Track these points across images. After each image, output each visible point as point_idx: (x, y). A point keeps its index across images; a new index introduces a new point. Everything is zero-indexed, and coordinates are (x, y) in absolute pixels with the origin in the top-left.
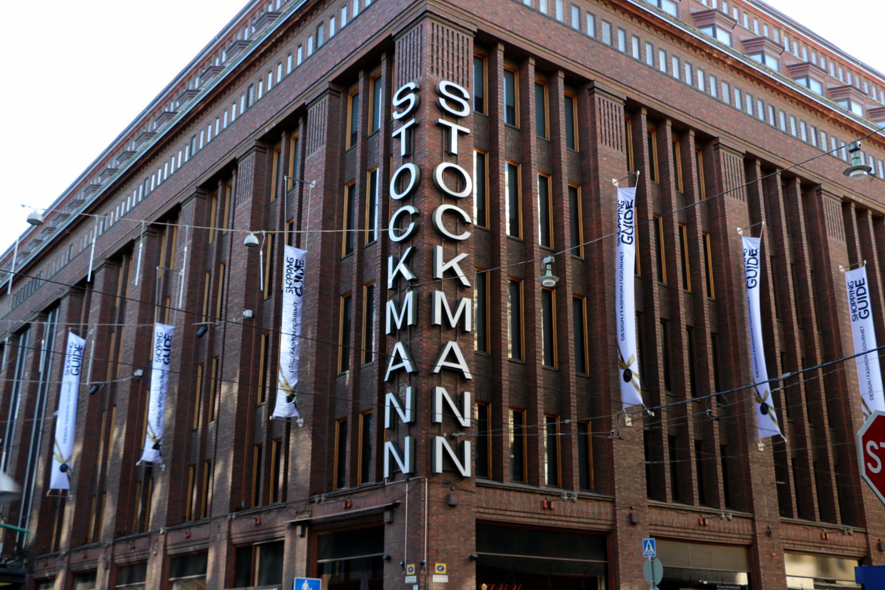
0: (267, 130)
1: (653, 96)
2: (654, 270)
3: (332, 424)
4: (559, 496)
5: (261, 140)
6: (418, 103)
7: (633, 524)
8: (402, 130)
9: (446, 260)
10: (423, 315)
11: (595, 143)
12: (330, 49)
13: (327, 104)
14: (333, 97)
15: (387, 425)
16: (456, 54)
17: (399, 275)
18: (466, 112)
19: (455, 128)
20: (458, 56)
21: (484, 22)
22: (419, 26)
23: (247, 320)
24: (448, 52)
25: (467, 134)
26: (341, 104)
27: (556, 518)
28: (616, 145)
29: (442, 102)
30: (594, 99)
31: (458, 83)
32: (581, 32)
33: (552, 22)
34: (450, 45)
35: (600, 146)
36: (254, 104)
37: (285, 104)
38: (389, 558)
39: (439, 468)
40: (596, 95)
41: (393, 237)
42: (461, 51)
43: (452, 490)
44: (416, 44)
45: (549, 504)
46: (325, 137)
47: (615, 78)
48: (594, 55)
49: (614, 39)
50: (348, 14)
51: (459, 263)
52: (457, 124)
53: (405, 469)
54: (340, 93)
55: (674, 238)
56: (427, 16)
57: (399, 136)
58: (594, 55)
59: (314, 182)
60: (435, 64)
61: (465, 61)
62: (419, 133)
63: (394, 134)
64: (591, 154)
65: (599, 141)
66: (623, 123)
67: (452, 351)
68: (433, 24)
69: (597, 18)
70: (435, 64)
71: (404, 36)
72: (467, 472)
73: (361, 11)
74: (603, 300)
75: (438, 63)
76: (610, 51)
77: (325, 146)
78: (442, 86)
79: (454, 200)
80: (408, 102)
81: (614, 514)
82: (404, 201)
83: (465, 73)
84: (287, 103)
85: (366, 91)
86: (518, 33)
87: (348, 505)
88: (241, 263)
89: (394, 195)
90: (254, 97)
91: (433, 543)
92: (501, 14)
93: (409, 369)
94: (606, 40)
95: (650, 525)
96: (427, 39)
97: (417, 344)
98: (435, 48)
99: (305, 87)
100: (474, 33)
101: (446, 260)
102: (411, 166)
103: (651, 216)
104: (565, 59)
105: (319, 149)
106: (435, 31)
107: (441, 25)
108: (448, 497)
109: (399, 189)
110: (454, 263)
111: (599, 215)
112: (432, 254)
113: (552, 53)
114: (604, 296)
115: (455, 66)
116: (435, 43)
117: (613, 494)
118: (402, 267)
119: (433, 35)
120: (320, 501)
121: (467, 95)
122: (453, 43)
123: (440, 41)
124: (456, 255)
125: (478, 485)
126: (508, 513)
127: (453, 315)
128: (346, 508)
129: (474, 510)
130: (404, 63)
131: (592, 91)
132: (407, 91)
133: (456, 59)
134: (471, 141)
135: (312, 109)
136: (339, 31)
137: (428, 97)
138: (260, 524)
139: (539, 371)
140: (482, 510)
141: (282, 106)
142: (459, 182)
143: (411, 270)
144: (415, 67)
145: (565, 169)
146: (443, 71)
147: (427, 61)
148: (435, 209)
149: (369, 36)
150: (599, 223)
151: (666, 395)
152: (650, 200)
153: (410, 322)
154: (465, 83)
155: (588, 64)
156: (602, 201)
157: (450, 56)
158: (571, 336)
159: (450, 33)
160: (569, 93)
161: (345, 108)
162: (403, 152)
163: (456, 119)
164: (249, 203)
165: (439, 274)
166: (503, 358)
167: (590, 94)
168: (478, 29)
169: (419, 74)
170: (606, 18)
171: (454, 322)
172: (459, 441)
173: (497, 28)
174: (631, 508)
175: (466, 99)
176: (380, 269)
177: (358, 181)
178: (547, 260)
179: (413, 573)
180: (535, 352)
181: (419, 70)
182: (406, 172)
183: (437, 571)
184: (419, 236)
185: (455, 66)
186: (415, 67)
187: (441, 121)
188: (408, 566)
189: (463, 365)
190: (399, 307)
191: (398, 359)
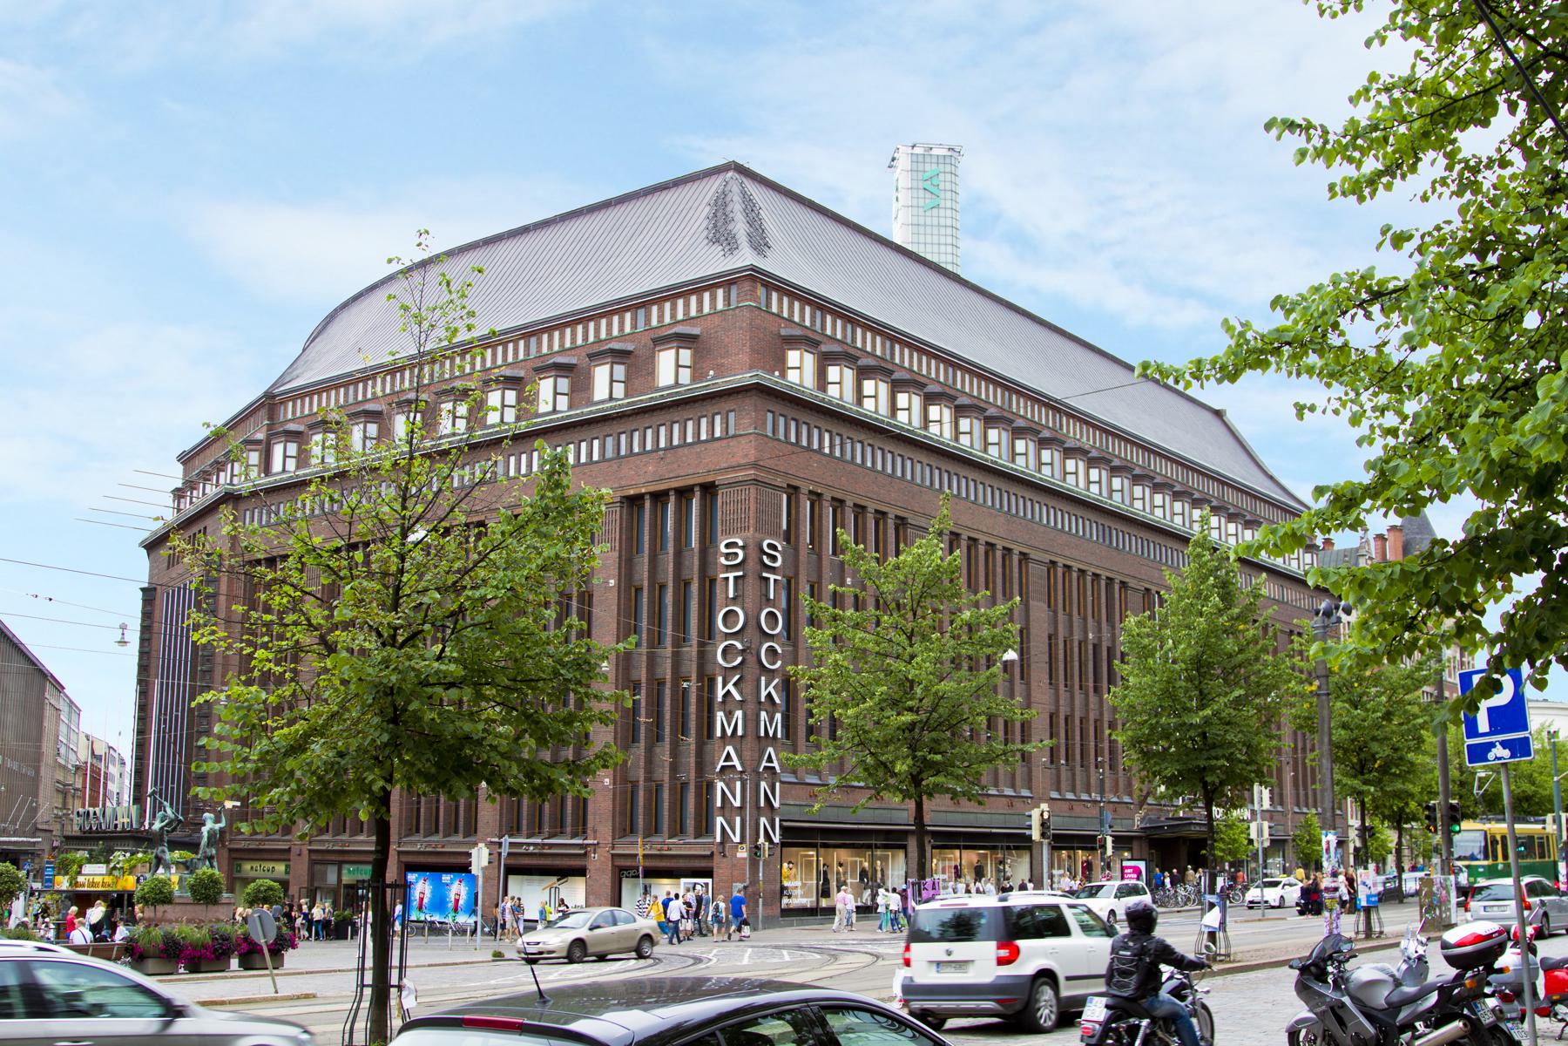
10: (751, 725)
18: (778, 564)
19: (772, 577)
57: (727, 579)
93: (739, 768)
110: (771, 689)
118: (730, 687)
153: (740, 732)
162: (731, 595)
163: (773, 570)
165: (763, 699)
189: (776, 764)
191: (728, 757)
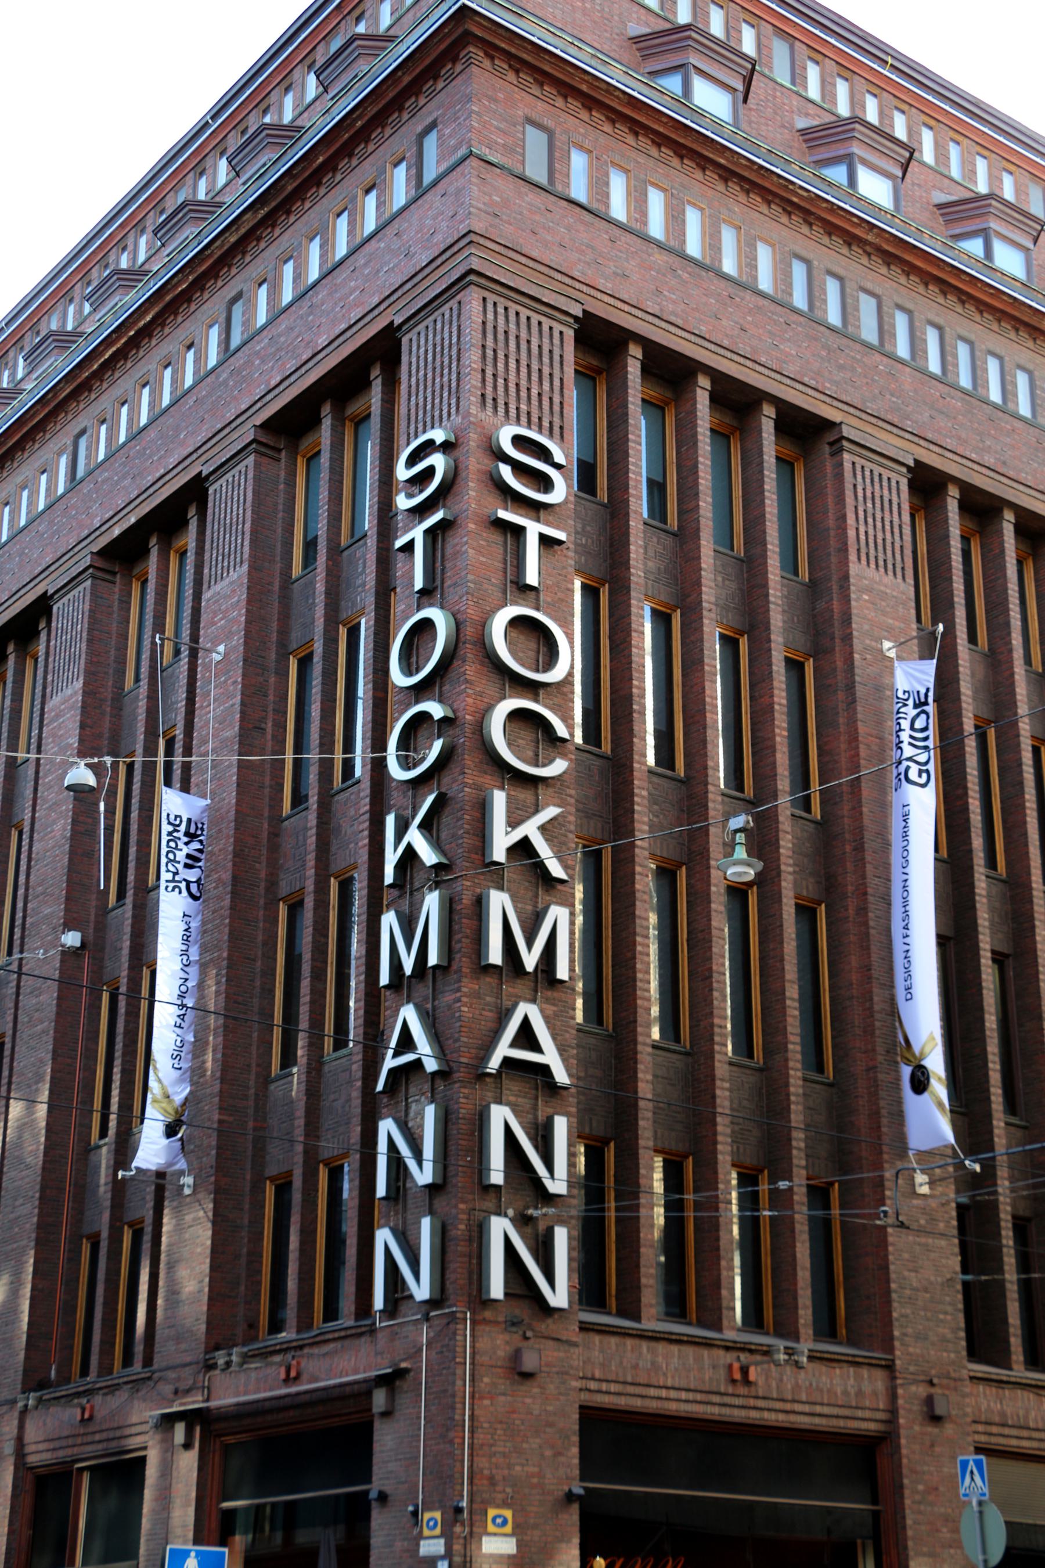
0: (117, 532)
1: (973, 456)
2: (977, 842)
3: (257, 1187)
4: (767, 1352)
5: (102, 553)
6: (451, 475)
7: (936, 1419)
8: (417, 534)
9: (513, 823)
10: (463, 944)
11: (845, 562)
12: (258, 353)
13: (251, 475)
14: (265, 460)
15: (381, 1191)
16: (535, 367)
17: (410, 855)
18: (558, 494)
19: (533, 529)
20: (540, 370)
21: (599, 295)
22: (453, 303)
23: (70, 955)
24: (518, 361)
25: (560, 542)
26: (282, 474)
27: (760, 1403)
28: (890, 566)
29: (506, 472)
30: (842, 464)
31: (540, 431)
32: (813, 317)
33: (748, 295)
34: (524, 346)
35: (854, 568)
36: (89, 473)
37: (158, 475)
38: (383, 1498)
39: (497, 1289)
40: (846, 456)
41: (396, 771)
42: (546, 360)
43: (526, 1338)
44: (446, 343)
45: (745, 1371)
46: (247, 549)
47: (889, 418)
48: (841, 368)
49: (885, 330)
50: (297, 277)
51: (543, 829)
52: (538, 520)
53: (421, 1290)
54: (279, 451)
55: (1021, 772)
56: (471, 283)
57: (409, 547)
58: (841, 368)
59: (221, 648)
60: (489, 389)
61: (557, 383)
62: (454, 541)
63: (399, 543)
64: (835, 588)
65: (853, 557)
66: (906, 518)
67: (526, 1023)
68: (484, 299)
69: (848, 284)
70: (489, 389)
71: (421, 327)
72: (559, 1297)
73: (325, 270)
74: (863, 910)
75: (495, 387)
76: (877, 357)
77: (245, 567)
78: (505, 438)
79: (532, 688)
80: (430, 471)
81: (893, 1396)
82: (420, 691)
83: (556, 408)
84: (162, 471)
85: (337, 446)
86: (672, 319)
87: (293, 1374)
88: (58, 827)
89: (398, 678)
90: (88, 457)
91: (482, 1462)
92: (635, 277)
94: (869, 332)
95: (975, 1422)
96: (472, 335)
97: (449, 1007)
98: (490, 353)
99: (200, 438)
100: (576, 318)
101: (513, 823)
102: (434, 613)
103: (969, 725)
104: (778, 377)
105: (234, 575)
106: (490, 316)
107: (502, 302)
108: (516, 1356)
109: (410, 662)
110: (530, 829)
111: (852, 722)
112: (483, 808)
113: (748, 363)
114: (865, 901)
115: (534, 392)
116: (490, 342)
117: (891, 1350)
118: (415, 837)
119: (484, 323)
120: (228, 1364)
121: (559, 457)
122: (529, 342)
123: (501, 337)
124: (537, 811)
125: (585, 1328)
126: (652, 1392)
127: (530, 943)
128: (287, 1380)
129: (576, 1384)
130: (421, 387)
131: (837, 445)
132: (428, 447)
133: (535, 377)
134: (569, 558)
135: (216, 486)
136: (277, 314)
137: (475, 462)
138: (91, 1418)
139: (721, 1069)
140: (593, 1385)
141: (150, 479)
142: (543, 649)
143: (436, 844)
144: (445, 394)
145: (777, 619)
146: (506, 404)
147: (472, 382)
148: (490, 708)
149: (343, 326)
150: (854, 739)
151: (1007, 1124)
152: (966, 689)
153: (433, 960)
154: (556, 430)
155: (830, 388)
156: (860, 691)
157: (524, 370)
158: (792, 992)
159: (523, 319)
160: (788, 452)
161: (291, 484)
162: (419, 584)
163: (536, 509)
164: (76, 693)
165: (499, 854)
166: (640, 1039)
167: (833, 454)
168: (584, 311)
169: (453, 410)
170: (869, 286)
171: (530, 960)
172: (542, 1226)
173: (627, 308)
174: (931, 1383)
175: (558, 467)
176: (366, 841)
177: (318, 647)
178: (737, 822)
179: (438, 1531)
180: (712, 1025)
181: (453, 401)
182: (426, 626)
183: (491, 1528)
184: (454, 769)
185: (534, 392)
186: (445, 394)
187: (502, 514)
188: (427, 1516)
189: (550, 1057)
190: (408, 924)
191: (406, 1042)
